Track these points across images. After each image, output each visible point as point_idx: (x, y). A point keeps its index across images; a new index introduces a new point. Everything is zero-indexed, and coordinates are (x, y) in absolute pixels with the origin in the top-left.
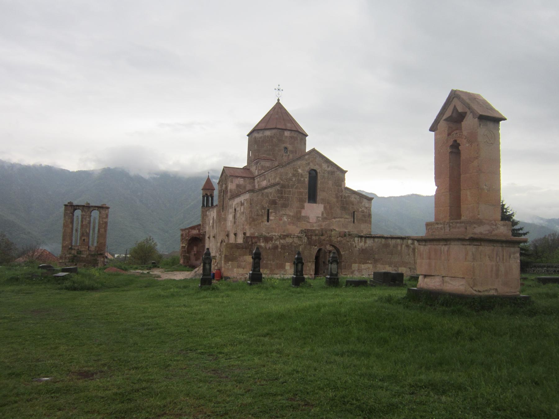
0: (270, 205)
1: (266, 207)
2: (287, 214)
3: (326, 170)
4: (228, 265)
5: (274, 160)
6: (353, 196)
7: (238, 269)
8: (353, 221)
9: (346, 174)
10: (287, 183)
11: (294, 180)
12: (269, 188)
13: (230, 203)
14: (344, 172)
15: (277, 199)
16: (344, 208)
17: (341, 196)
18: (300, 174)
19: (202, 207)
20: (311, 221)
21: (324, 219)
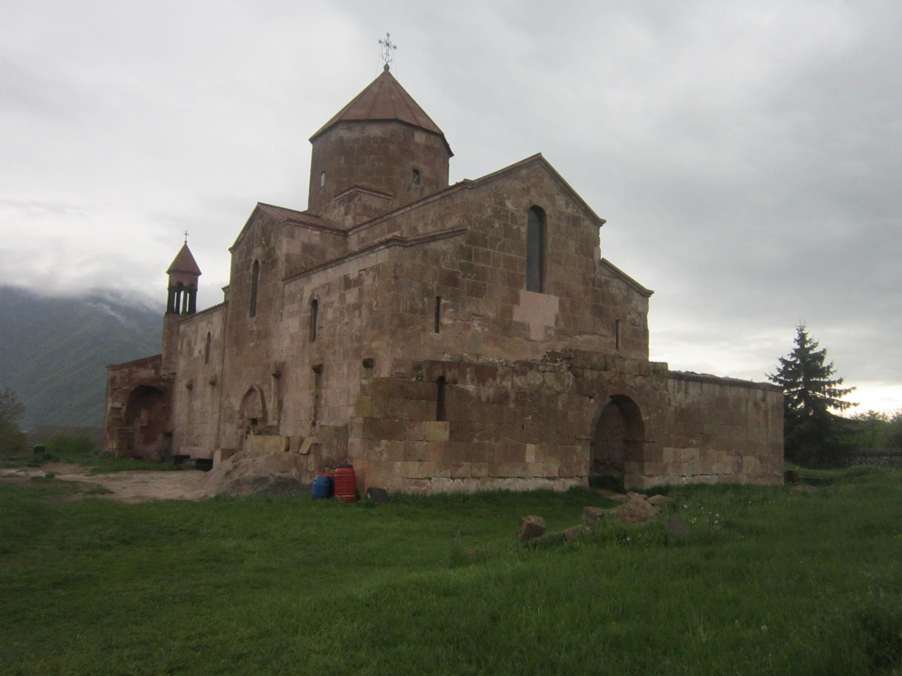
0: (442, 286)
1: (433, 290)
2: (481, 313)
3: (564, 213)
4: (377, 449)
5: (391, 196)
6: (616, 283)
7: (405, 462)
8: (615, 342)
9: (602, 229)
10: (481, 232)
11: (497, 225)
12: (439, 239)
13: (291, 287)
14: (599, 223)
15: (459, 271)
16: (598, 311)
17: (593, 280)
18: (510, 214)
19: (166, 314)
20: (533, 337)
21: (561, 334)
